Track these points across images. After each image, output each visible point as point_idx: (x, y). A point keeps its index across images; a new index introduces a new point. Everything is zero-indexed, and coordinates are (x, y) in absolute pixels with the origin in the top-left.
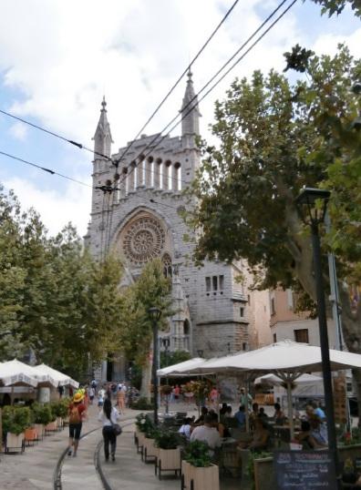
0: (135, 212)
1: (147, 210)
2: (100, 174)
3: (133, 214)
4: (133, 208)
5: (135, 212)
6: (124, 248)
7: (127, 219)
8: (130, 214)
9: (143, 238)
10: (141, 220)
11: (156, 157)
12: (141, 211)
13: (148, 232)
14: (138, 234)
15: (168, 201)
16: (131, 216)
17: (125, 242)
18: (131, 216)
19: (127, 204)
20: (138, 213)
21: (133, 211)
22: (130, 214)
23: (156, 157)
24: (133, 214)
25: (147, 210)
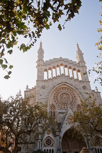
0: (61, 84)
1: (67, 84)
2: (42, 65)
3: (60, 85)
4: (61, 82)
5: (61, 84)
6: (54, 99)
7: (57, 86)
8: (59, 84)
9: (65, 96)
10: (63, 88)
11: (69, 66)
12: (64, 84)
13: (67, 94)
14: (62, 94)
15: (77, 83)
16: (59, 85)
17: (54, 97)
18: (59, 85)
19: (56, 80)
20: (62, 85)
21: (60, 84)
22: (59, 84)
23: (69, 66)
24: (60, 85)
25: (67, 84)
